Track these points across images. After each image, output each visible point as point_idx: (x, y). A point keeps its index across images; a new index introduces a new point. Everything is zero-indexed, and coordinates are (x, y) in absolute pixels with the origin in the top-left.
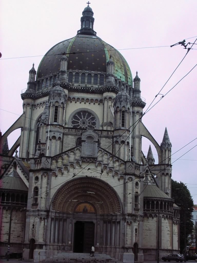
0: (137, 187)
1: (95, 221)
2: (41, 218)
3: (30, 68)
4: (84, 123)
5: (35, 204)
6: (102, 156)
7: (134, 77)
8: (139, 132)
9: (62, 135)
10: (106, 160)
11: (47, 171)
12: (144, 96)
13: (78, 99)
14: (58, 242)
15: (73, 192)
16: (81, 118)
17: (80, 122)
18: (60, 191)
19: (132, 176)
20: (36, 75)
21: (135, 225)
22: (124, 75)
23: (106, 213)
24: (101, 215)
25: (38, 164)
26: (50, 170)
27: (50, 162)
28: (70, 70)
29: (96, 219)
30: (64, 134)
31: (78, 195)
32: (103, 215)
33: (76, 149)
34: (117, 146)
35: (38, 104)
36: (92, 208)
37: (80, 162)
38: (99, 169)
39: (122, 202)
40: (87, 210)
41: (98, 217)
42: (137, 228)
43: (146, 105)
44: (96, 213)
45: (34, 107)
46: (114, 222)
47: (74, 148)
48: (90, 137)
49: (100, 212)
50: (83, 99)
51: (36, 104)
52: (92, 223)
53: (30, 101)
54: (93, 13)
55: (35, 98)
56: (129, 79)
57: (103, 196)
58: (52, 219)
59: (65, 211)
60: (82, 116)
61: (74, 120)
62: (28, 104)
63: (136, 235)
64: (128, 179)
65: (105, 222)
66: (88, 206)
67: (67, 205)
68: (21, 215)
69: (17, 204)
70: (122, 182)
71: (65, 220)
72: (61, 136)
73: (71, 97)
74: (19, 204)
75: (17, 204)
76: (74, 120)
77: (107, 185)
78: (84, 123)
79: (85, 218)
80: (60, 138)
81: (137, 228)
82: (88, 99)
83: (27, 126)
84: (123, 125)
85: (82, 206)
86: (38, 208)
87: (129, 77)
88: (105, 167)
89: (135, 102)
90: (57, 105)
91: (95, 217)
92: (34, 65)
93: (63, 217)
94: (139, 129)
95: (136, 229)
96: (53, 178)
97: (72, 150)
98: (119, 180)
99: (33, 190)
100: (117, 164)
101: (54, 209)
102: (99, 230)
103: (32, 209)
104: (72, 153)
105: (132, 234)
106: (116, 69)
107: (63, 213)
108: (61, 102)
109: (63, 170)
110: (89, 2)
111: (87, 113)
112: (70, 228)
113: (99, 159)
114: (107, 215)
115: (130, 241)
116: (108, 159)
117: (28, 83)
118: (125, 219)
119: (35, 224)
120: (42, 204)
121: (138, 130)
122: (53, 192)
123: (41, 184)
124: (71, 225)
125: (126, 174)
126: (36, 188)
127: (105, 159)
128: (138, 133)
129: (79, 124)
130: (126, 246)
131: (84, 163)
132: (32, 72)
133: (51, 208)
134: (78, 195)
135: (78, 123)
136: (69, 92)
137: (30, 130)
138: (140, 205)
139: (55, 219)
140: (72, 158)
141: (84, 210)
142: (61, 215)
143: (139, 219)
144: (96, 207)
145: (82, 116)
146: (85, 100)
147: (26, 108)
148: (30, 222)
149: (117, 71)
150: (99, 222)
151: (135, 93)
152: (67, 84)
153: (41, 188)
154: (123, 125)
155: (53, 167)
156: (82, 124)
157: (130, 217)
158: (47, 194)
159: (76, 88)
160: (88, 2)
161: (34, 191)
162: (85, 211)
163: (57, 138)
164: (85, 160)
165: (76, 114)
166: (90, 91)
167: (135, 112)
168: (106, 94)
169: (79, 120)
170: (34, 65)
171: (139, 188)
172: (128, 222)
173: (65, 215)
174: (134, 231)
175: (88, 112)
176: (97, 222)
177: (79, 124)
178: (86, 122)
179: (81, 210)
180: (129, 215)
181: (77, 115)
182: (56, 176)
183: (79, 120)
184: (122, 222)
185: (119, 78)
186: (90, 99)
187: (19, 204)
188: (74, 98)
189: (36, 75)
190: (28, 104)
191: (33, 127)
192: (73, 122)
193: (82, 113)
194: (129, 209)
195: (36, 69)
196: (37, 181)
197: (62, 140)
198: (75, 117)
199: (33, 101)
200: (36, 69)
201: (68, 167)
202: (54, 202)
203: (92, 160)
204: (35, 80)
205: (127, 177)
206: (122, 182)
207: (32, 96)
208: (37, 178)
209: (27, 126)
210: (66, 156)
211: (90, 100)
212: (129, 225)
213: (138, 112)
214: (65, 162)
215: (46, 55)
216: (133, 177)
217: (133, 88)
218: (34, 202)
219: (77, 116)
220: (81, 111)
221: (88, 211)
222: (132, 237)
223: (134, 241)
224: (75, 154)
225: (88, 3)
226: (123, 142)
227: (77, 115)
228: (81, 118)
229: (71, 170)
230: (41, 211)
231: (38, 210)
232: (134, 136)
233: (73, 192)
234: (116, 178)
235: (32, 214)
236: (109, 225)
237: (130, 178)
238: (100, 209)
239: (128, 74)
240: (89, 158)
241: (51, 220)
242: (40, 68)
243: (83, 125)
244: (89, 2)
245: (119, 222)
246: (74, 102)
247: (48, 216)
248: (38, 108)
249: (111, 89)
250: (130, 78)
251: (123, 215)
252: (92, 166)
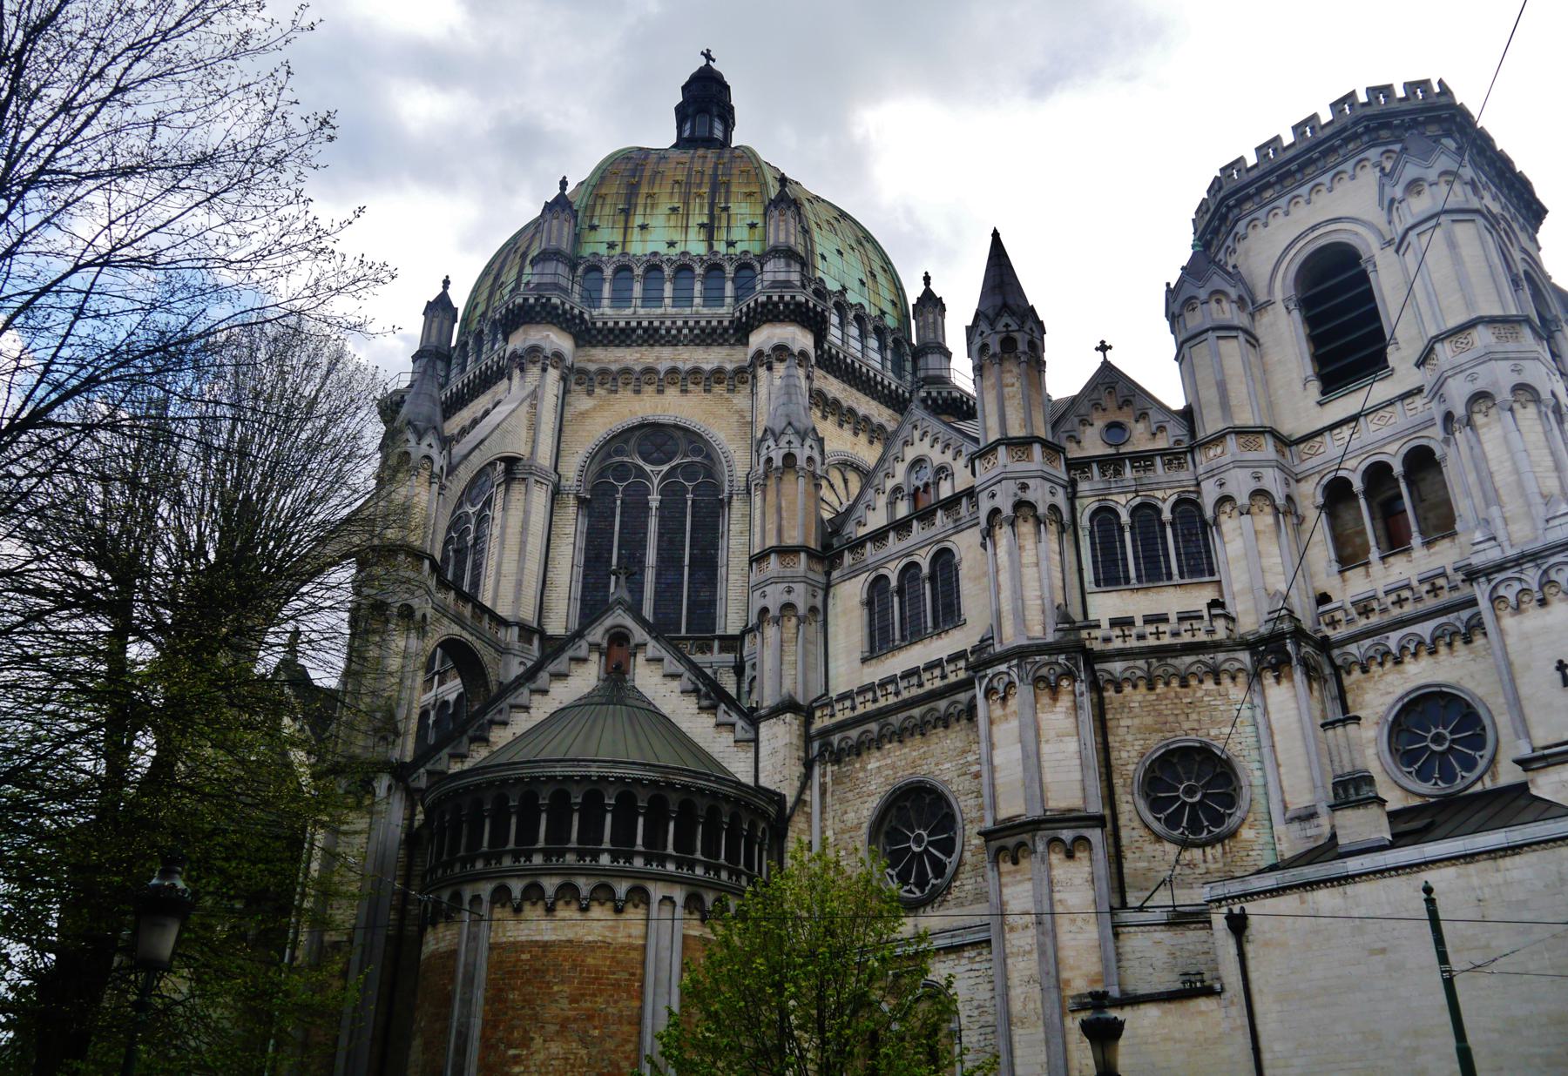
20: (457, 326)
54: (728, 88)
92: (446, 283)
117: (415, 358)
132: (439, 308)
136: (577, 345)
149: (823, 257)
152: (563, 304)
168: (764, 337)
170: (446, 283)
189: (457, 326)
195: (460, 299)
200: (460, 299)
204: (453, 343)
217: (914, 341)
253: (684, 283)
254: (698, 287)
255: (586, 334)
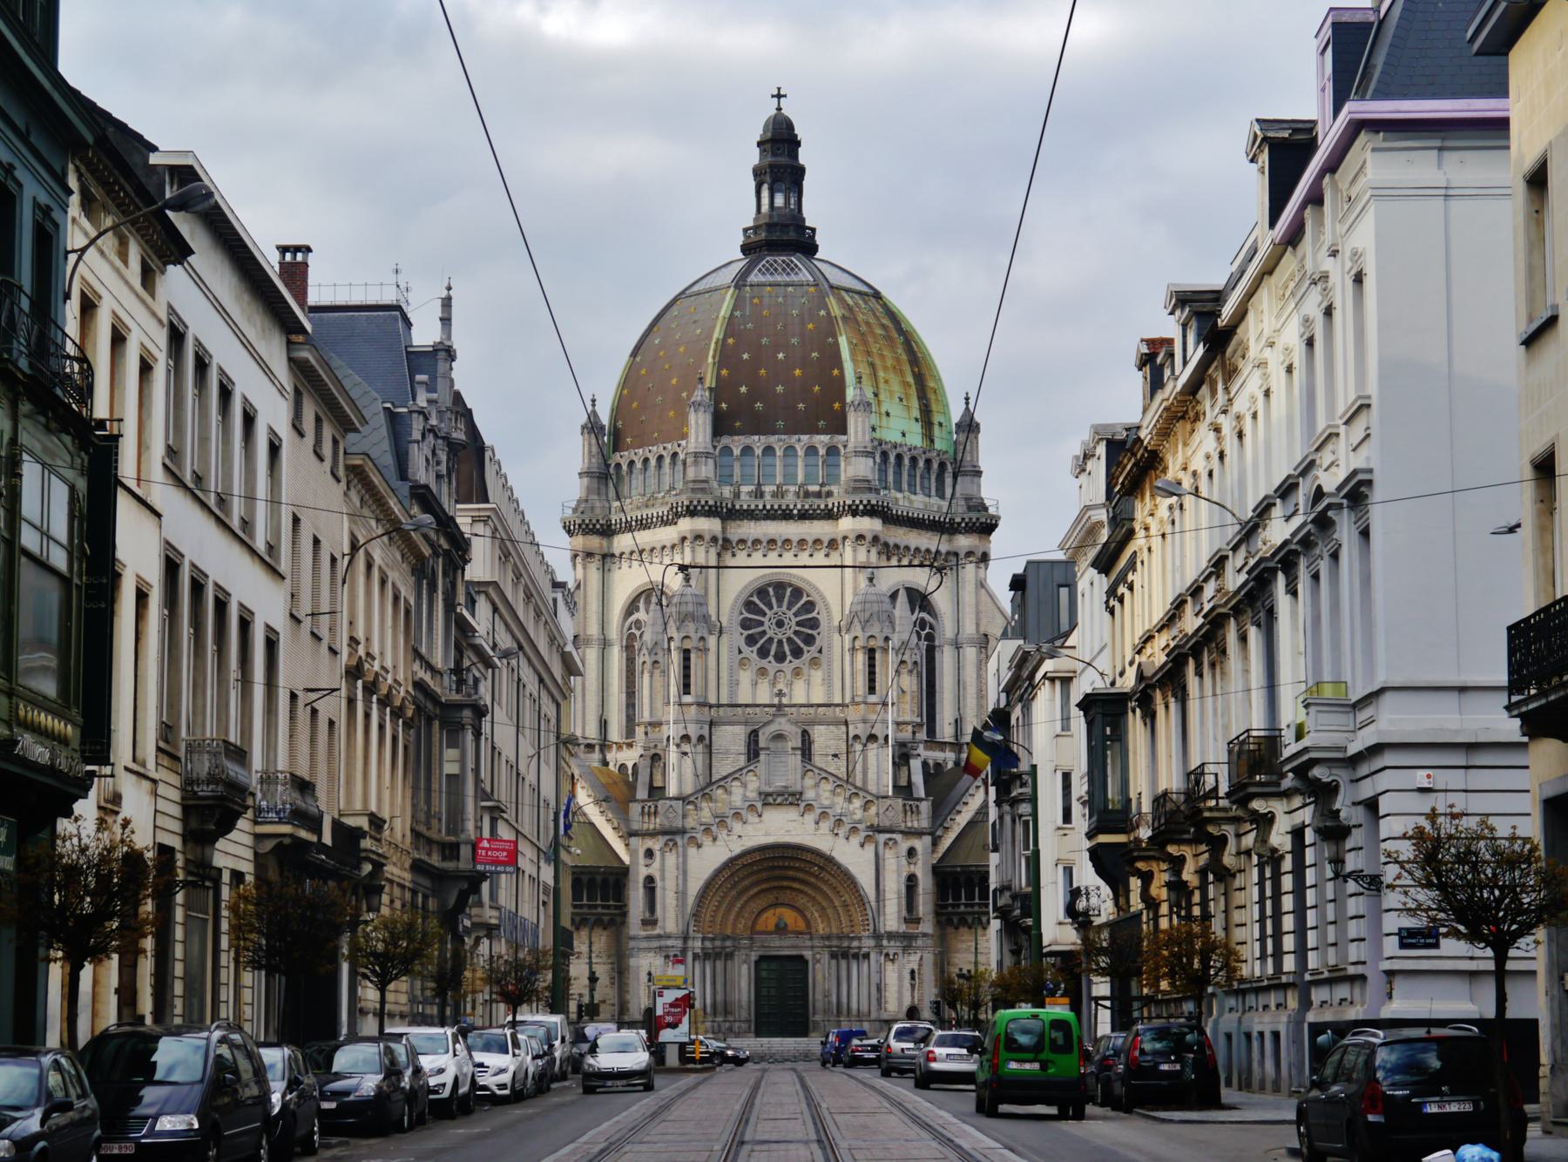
0: (914, 860)
1: (808, 954)
2: (667, 957)
3: (584, 419)
4: (780, 624)
5: (650, 922)
6: (817, 785)
7: (956, 414)
8: (978, 625)
9: (707, 727)
10: (827, 794)
11: (671, 834)
12: (991, 491)
13: (757, 542)
14: (715, 1013)
15: (746, 882)
16: (771, 608)
17: (765, 620)
18: (708, 885)
19: (894, 836)
21: (913, 961)
22: (917, 420)
23: (835, 931)
24: (822, 938)
25: (649, 814)
26: (683, 832)
27: (680, 812)
28: (726, 440)
29: (812, 947)
30: (711, 724)
31: (759, 888)
32: (828, 938)
33: (745, 771)
34: (858, 747)
35: (622, 554)
36: (800, 919)
37: (759, 805)
38: (810, 818)
39: (873, 904)
40: (786, 925)
41: (816, 943)
42: (916, 968)
43: (1001, 523)
44: (809, 932)
45: (609, 559)
46: (856, 956)
47: (741, 769)
48: (779, 737)
49: (821, 928)
50: (772, 542)
51: (617, 553)
52: (801, 958)
53: (595, 542)
55: (607, 531)
56: (936, 429)
57: (825, 888)
58: (696, 957)
59: (729, 932)
60: (774, 600)
61: (747, 615)
62: (589, 555)
63: (913, 986)
64: (886, 844)
65: (833, 956)
66: (789, 916)
67: (732, 917)
68: (603, 939)
69: (590, 907)
70: (870, 848)
71: (729, 956)
72: (706, 732)
73: (729, 536)
74: (596, 907)
75: (590, 907)
76: (747, 615)
77: (830, 860)
78: (780, 624)
79: (782, 946)
80: (701, 738)
81: (916, 968)
82: (787, 541)
83: (593, 630)
84: (872, 690)
85: (769, 919)
86: (658, 931)
87: (936, 418)
88: (824, 815)
89: (958, 520)
90: (688, 645)
91: (808, 943)
93: (723, 948)
94: (978, 613)
95: (913, 972)
96: (692, 851)
97: (734, 776)
98: (862, 845)
99: (641, 885)
100: (857, 803)
101: (698, 932)
102: (819, 977)
103: (643, 933)
104: (736, 783)
105: (900, 987)
106: (883, 410)
107: (727, 938)
108: (699, 635)
109: (714, 828)
110: (779, 89)
111: (789, 590)
112: (743, 978)
113: (810, 794)
114: (839, 938)
115: (896, 1002)
116: (833, 792)
118: (879, 946)
119: (653, 971)
120: (670, 919)
121: (973, 616)
122: (694, 887)
123: (663, 870)
124: (744, 968)
125: (880, 830)
126: (650, 880)
127: (822, 794)
128: (974, 627)
129: (765, 627)
130: (885, 1016)
131: (769, 808)
132: (592, 427)
133: (691, 928)
134: (759, 888)
135: (762, 624)
137: (605, 644)
138: (924, 905)
139: (706, 956)
140: (736, 796)
141: (777, 926)
142: (718, 943)
143: (920, 942)
144: (809, 916)
145: (774, 600)
146: (779, 544)
147: (584, 568)
148: (638, 967)
149: (888, 414)
150: (818, 956)
151: (959, 479)
153: (663, 879)
154: (872, 690)
155: (690, 822)
156: (774, 626)
157: (892, 943)
158: (681, 894)
159: (745, 507)
160: (776, 93)
161: (645, 887)
162: (781, 929)
163: (694, 740)
164: (770, 800)
165: (751, 596)
166: (795, 512)
167: (962, 555)
169: (764, 614)
171: (920, 863)
172: (887, 955)
173: (728, 943)
174: (907, 976)
175: (790, 585)
176: (814, 955)
177: (765, 627)
178: (786, 621)
179: (771, 927)
180: (891, 936)
181: (755, 599)
182: (699, 846)
183: (764, 614)
184: (873, 956)
185: (897, 438)
186: (795, 539)
187: (596, 907)
188: (742, 541)
190: (589, 555)
191: (614, 632)
192: (745, 624)
193: (771, 590)
194: (892, 919)
195: (605, 419)
196: (649, 861)
197: (707, 742)
198: (749, 605)
199: (605, 542)
200: (605, 419)
201: (728, 820)
202: (696, 915)
203: (791, 798)
205: (882, 838)
206: (870, 848)
207: (602, 525)
208: (649, 853)
209: (593, 630)
210: (720, 791)
211: (795, 544)
212: (893, 961)
213: (969, 554)
214: (720, 808)
215: (634, 354)
216: (898, 837)
218: (647, 915)
219: (758, 602)
220: (769, 585)
221: (790, 929)
222: (900, 992)
223: (907, 1003)
224: (744, 785)
225: (779, 96)
226: (872, 738)
227: (755, 599)
228: (771, 608)
229: (737, 827)
230: (668, 937)
231: (659, 937)
232: (960, 640)
233: (746, 882)
234: (855, 840)
235: (644, 944)
236: (843, 963)
237: (890, 839)
238: (819, 920)
239: (934, 407)
240: (780, 794)
241: (694, 960)
242: (618, 410)
243: (777, 630)
244: (779, 89)
245: (867, 956)
246: (745, 553)
247: (684, 950)
248: (625, 565)
249: (861, 507)
250: (940, 424)
251: (877, 936)
252: (791, 814)
253: (790, 460)
254: (800, 463)
255: (729, 514)
